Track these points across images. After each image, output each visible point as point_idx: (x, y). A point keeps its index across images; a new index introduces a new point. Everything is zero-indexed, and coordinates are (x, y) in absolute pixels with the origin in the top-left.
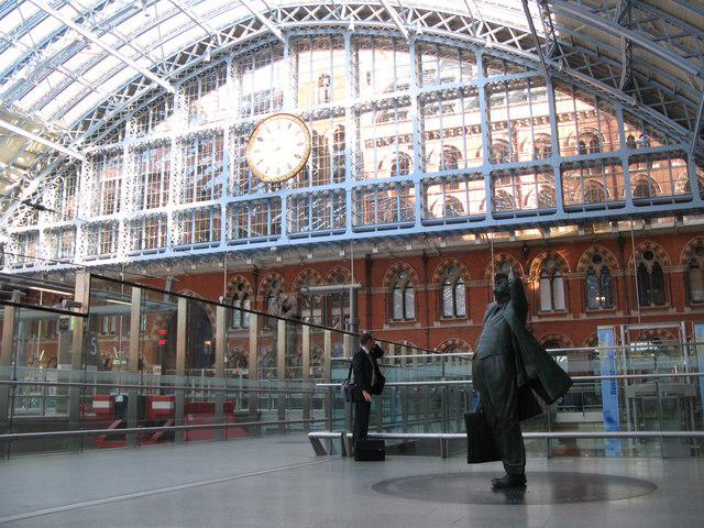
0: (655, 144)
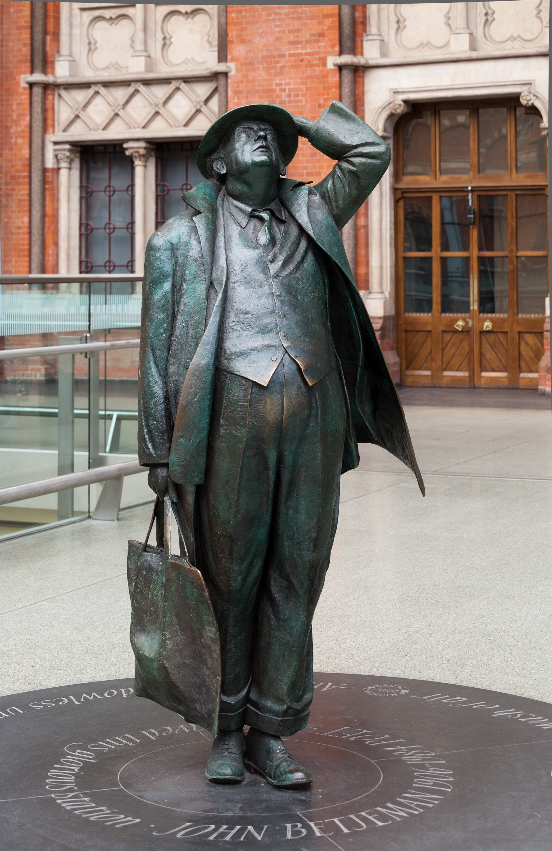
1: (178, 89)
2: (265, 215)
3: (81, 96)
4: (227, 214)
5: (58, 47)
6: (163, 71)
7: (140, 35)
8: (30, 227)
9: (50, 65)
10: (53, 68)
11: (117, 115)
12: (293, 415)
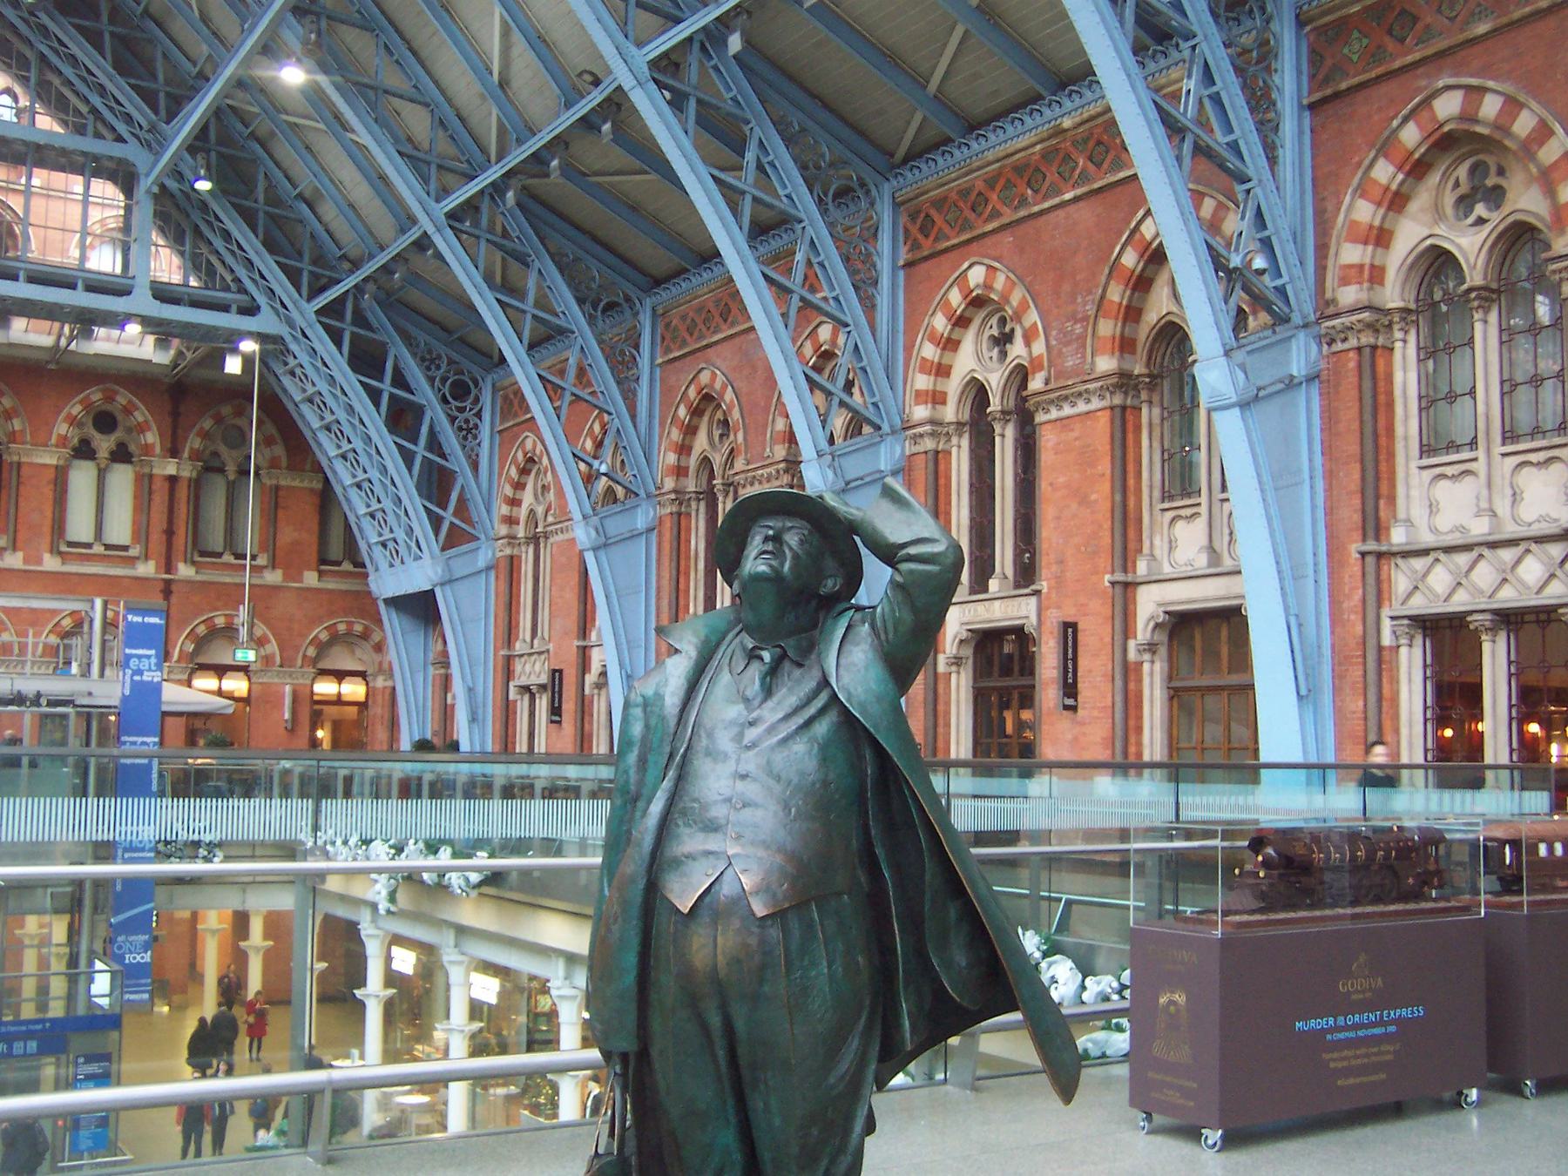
0: (46, 122)
1: (1528, 551)
2: (766, 656)
3: (1419, 564)
4: (729, 651)
5: (1394, 511)
6: (1510, 530)
7: (1485, 492)
8: (1365, 712)
9: (1383, 532)
10: (1388, 536)
11: (1459, 584)
12: (735, 961)
